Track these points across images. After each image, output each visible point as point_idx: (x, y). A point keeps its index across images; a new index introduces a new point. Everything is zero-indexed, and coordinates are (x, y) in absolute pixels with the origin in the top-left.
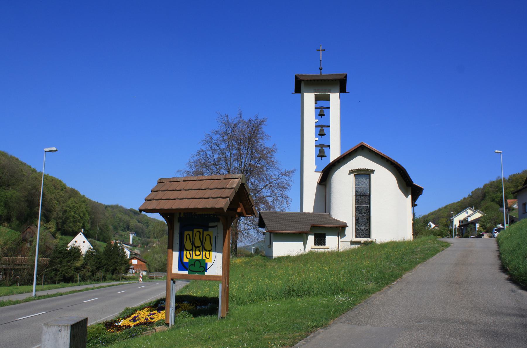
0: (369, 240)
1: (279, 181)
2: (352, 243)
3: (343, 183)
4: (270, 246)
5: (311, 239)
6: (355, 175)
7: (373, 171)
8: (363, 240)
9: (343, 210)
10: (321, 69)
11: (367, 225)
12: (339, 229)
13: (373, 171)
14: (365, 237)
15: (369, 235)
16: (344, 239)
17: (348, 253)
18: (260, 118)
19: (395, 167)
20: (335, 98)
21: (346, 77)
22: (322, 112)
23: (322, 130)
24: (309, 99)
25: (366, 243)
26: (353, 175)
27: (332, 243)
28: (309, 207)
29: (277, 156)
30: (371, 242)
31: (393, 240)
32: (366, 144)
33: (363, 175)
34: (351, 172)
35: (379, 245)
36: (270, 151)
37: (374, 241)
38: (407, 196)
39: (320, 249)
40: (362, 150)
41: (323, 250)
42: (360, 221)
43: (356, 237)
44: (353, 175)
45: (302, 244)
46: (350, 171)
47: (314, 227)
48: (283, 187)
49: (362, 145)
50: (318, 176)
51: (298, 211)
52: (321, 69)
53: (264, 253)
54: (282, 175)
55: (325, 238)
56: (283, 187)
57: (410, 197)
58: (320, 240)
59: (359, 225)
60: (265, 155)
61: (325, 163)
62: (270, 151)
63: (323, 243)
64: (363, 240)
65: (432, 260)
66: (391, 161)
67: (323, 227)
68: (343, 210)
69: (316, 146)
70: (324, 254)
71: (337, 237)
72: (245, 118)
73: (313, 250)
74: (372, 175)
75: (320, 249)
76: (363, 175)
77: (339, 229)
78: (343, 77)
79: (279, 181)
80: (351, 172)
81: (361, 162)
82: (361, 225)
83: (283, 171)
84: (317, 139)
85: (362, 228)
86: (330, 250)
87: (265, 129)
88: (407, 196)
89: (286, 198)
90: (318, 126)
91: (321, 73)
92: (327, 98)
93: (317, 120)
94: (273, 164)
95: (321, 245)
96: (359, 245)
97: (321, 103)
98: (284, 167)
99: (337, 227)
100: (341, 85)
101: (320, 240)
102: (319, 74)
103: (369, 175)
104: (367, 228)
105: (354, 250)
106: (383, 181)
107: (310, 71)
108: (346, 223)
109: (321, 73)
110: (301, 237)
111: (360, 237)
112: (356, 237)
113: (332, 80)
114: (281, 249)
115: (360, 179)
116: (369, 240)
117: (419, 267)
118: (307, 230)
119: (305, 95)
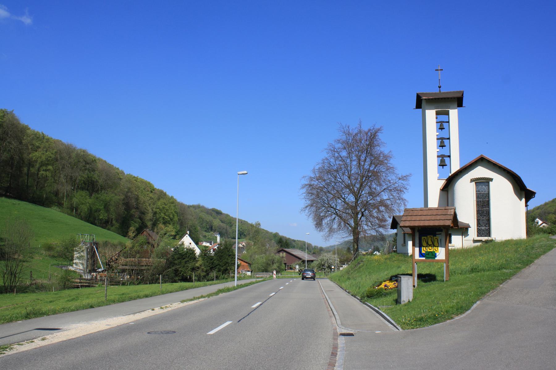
0: (490, 238)
1: (397, 185)
2: (475, 241)
7: (491, 180)
8: (484, 239)
9: (467, 213)
10: (440, 87)
12: (463, 230)
13: (491, 180)
14: (486, 236)
15: (489, 234)
16: (467, 238)
18: (377, 127)
20: (454, 113)
21: (463, 95)
22: (442, 126)
23: (443, 142)
24: (431, 114)
25: (486, 242)
26: (474, 183)
29: (392, 162)
30: (492, 241)
34: (472, 181)
36: (386, 157)
38: (521, 199)
40: (482, 161)
42: (481, 222)
43: (478, 236)
44: (474, 183)
46: (471, 180)
48: (400, 191)
52: (440, 87)
54: (400, 179)
56: (401, 191)
57: (524, 200)
60: (379, 161)
62: (386, 157)
64: (484, 239)
68: (467, 213)
69: (438, 156)
72: (365, 128)
74: (490, 182)
76: (483, 183)
77: (463, 230)
78: (460, 95)
79: (397, 185)
80: (472, 181)
81: (481, 172)
82: (482, 226)
83: (400, 176)
84: (438, 150)
85: (483, 228)
87: (381, 136)
88: (521, 199)
89: (403, 200)
91: (440, 91)
92: (447, 113)
93: (438, 134)
94: (389, 169)
97: (443, 118)
98: (401, 171)
100: (459, 101)
102: (438, 92)
103: (489, 183)
104: (487, 228)
105: (476, 247)
106: (501, 188)
107: (430, 89)
109: (440, 91)
111: (481, 236)
112: (478, 236)
113: (451, 98)
117: (543, 257)
119: (427, 111)
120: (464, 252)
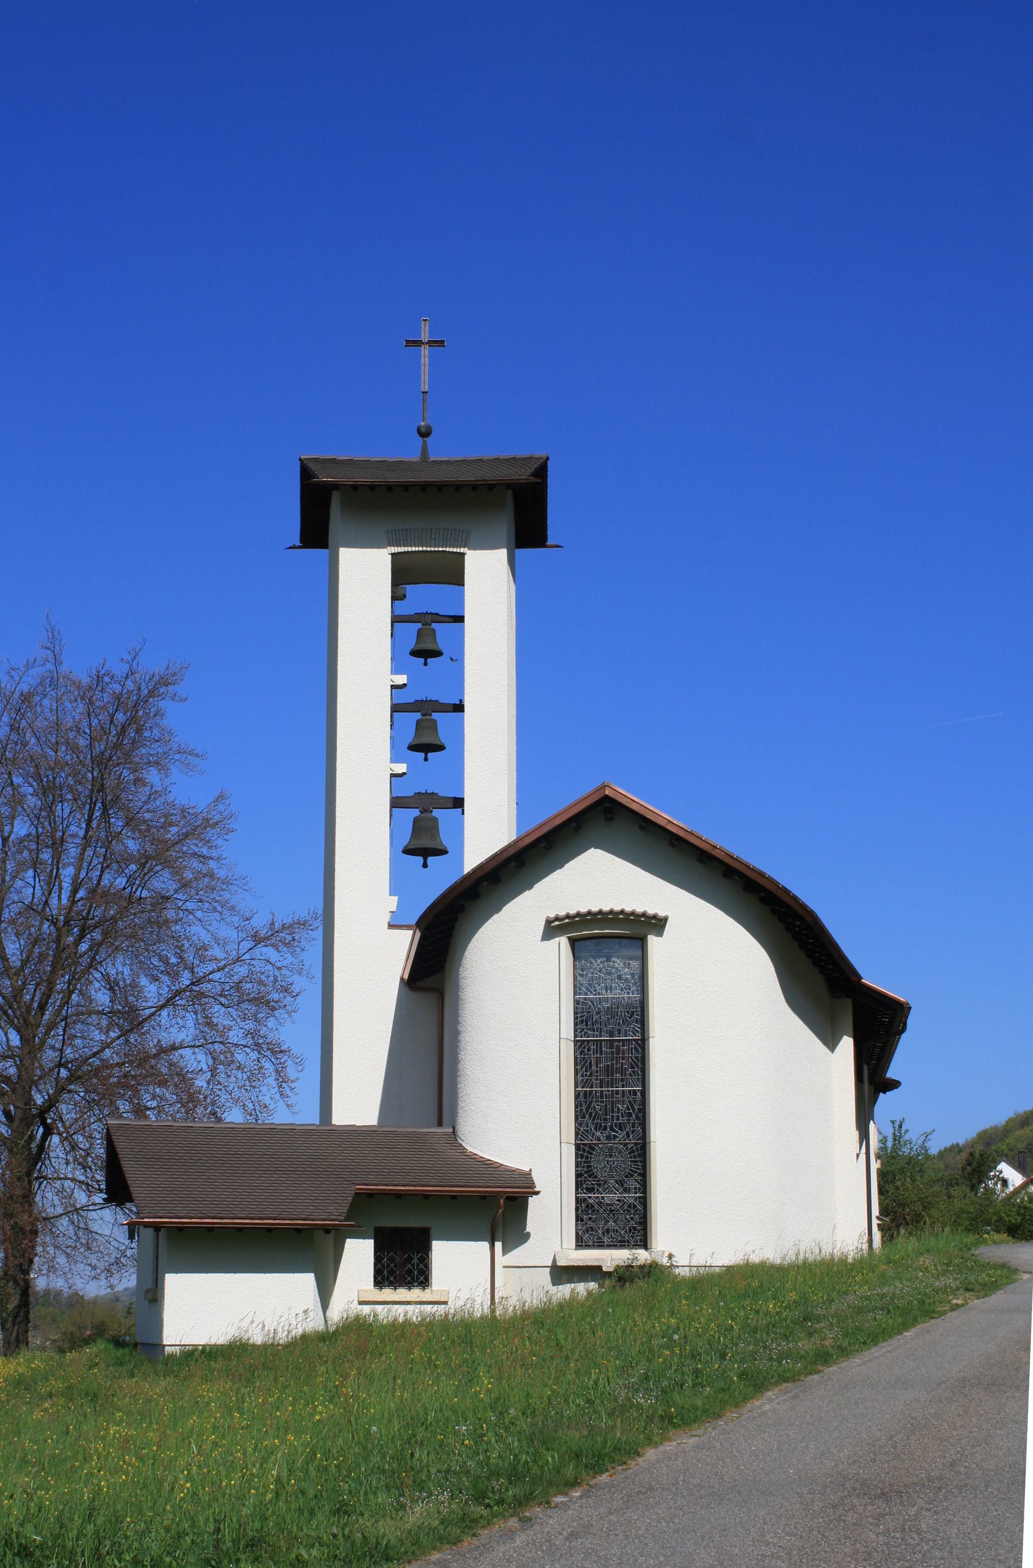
0: (642, 1256)
1: (241, 970)
2: (561, 1273)
3: (518, 979)
4: (152, 1295)
5: (359, 1255)
6: (573, 942)
7: (657, 924)
8: (610, 1258)
9: (518, 1112)
10: (424, 433)
11: (633, 1183)
12: (497, 1208)
13: (657, 924)
14: (622, 1244)
15: (639, 1234)
16: (520, 1255)
17: (537, 1321)
18: (151, 664)
19: (763, 900)
20: (488, 574)
21: (542, 471)
22: (427, 637)
23: (427, 724)
24: (364, 573)
25: (624, 1275)
26: (563, 941)
27: (462, 1272)
28: (358, 1099)
29: (234, 853)
30: (651, 1270)
31: (755, 1259)
32: (625, 792)
33: (610, 940)
34: (553, 928)
35: (684, 1281)
36: (200, 827)
37: (665, 1261)
38: (831, 1043)
39: (403, 1305)
40: (603, 820)
41: (413, 1313)
42: (599, 1165)
43: (581, 1243)
44: (563, 941)
45: (306, 1282)
46: (549, 922)
47: (370, 1195)
48: (260, 1000)
49: (607, 798)
50: (399, 948)
51: (308, 1116)
52: (424, 433)
53: (130, 1335)
54: (258, 940)
55: (427, 1249)
56: (260, 1001)
57: (847, 1044)
58: (403, 1262)
59: (591, 1182)
60: (174, 845)
61: (436, 880)
62: (200, 827)
63: (421, 1277)
64: (610, 1258)
65: (857, 1366)
66: (742, 875)
67: (418, 1196)
68: (518, 1112)
69: (396, 803)
70: (428, 1325)
71: (485, 1245)
72: (79, 666)
73: (366, 1309)
74: (652, 940)
75: (403, 1305)
76: (610, 940)
77: (497, 1208)
78: (524, 474)
79: (241, 970)
80: (553, 928)
81: (600, 879)
82: (602, 1184)
83: (260, 923)
84: (401, 768)
85: (609, 1197)
86: (453, 1306)
87: (176, 719)
88: (831, 1043)
89: (276, 1051)
90: (398, 710)
91: (424, 451)
92: (453, 574)
93: (401, 679)
94: (207, 886)
95: (409, 1285)
96: (593, 1285)
97: (424, 597)
98: (267, 902)
99: (483, 1197)
100: (521, 508)
101: (403, 1262)
102: (416, 458)
103: (642, 941)
104: (631, 1197)
105: (567, 1307)
106: (709, 974)
107: (376, 441)
108: (528, 1175)
109: (424, 451)
110: (306, 1247)
111: (600, 1245)
112: (581, 1243)
113: (474, 487)
114: (206, 1308)
115: (598, 963)
116: (642, 1256)
117: (771, 1403)
118: (335, 1211)
119: (346, 554)
120: (462, 1338)
